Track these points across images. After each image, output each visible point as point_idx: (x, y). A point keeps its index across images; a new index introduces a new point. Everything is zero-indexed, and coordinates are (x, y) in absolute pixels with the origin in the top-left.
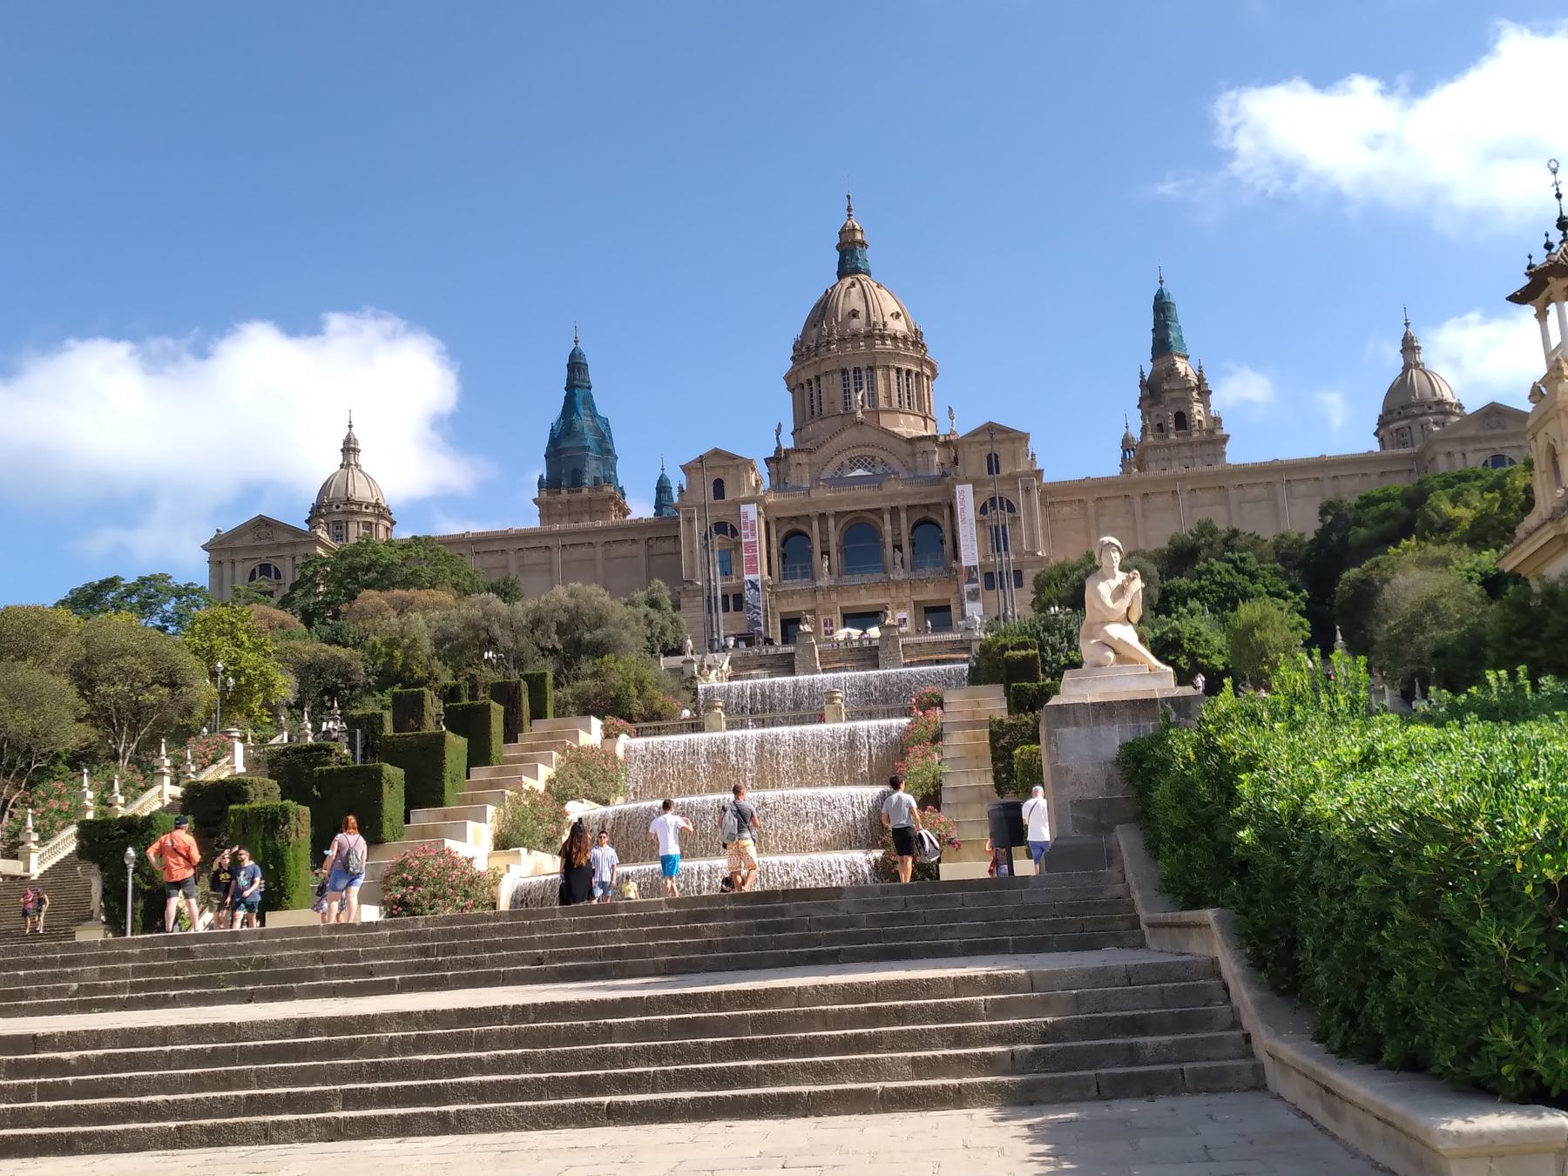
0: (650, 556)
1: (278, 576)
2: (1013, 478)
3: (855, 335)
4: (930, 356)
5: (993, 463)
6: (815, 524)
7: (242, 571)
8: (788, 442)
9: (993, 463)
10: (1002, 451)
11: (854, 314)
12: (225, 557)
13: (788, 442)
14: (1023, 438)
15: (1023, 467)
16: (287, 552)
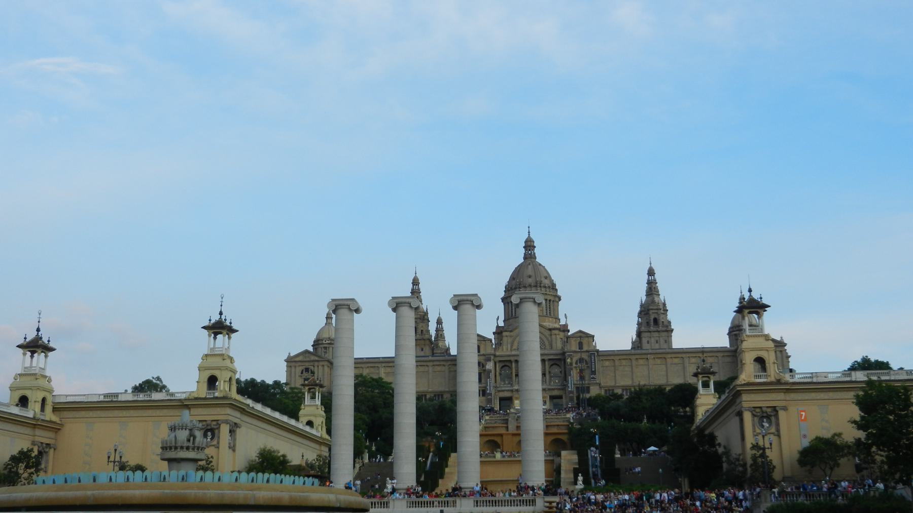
0: (450, 372)
1: (313, 373)
2: (587, 351)
3: (530, 286)
4: (559, 293)
5: (581, 345)
6: (514, 364)
7: (299, 370)
8: (501, 324)
9: (581, 345)
10: (585, 341)
11: (530, 277)
12: (293, 364)
13: (501, 324)
14: (593, 337)
15: (591, 348)
16: (316, 364)
